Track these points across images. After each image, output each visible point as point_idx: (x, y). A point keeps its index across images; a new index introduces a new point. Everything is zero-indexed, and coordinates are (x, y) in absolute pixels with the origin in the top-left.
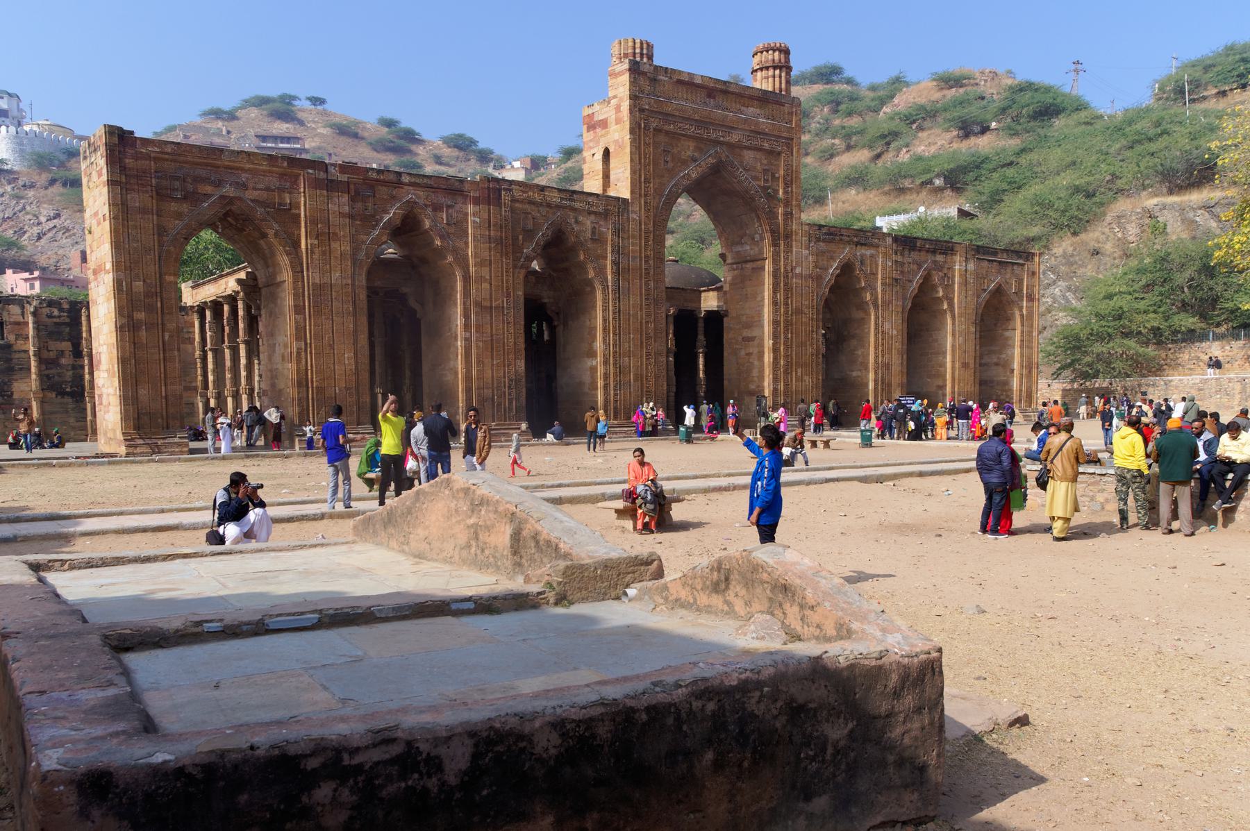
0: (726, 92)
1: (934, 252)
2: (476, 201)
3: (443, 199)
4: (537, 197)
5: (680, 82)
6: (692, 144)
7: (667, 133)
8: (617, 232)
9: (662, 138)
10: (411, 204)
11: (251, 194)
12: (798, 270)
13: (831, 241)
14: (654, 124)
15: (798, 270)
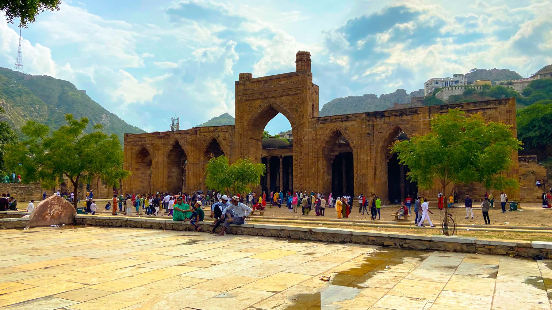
0: (271, 79)
1: (401, 115)
2: (191, 135)
3: (184, 136)
4: (207, 130)
5: (253, 82)
6: (259, 101)
7: (249, 100)
8: (231, 136)
9: (248, 102)
10: (176, 138)
11: (147, 142)
12: (306, 138)
13: (327, 123)
14: (244, 98)
15: (306, 138)
